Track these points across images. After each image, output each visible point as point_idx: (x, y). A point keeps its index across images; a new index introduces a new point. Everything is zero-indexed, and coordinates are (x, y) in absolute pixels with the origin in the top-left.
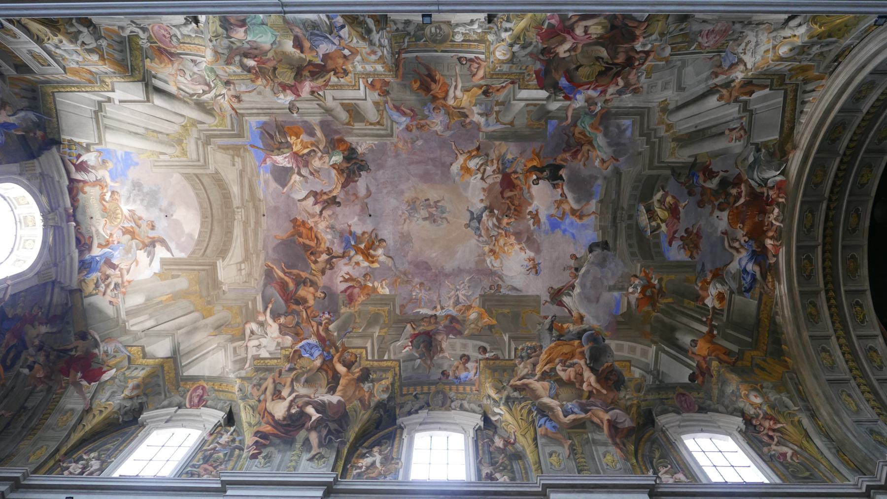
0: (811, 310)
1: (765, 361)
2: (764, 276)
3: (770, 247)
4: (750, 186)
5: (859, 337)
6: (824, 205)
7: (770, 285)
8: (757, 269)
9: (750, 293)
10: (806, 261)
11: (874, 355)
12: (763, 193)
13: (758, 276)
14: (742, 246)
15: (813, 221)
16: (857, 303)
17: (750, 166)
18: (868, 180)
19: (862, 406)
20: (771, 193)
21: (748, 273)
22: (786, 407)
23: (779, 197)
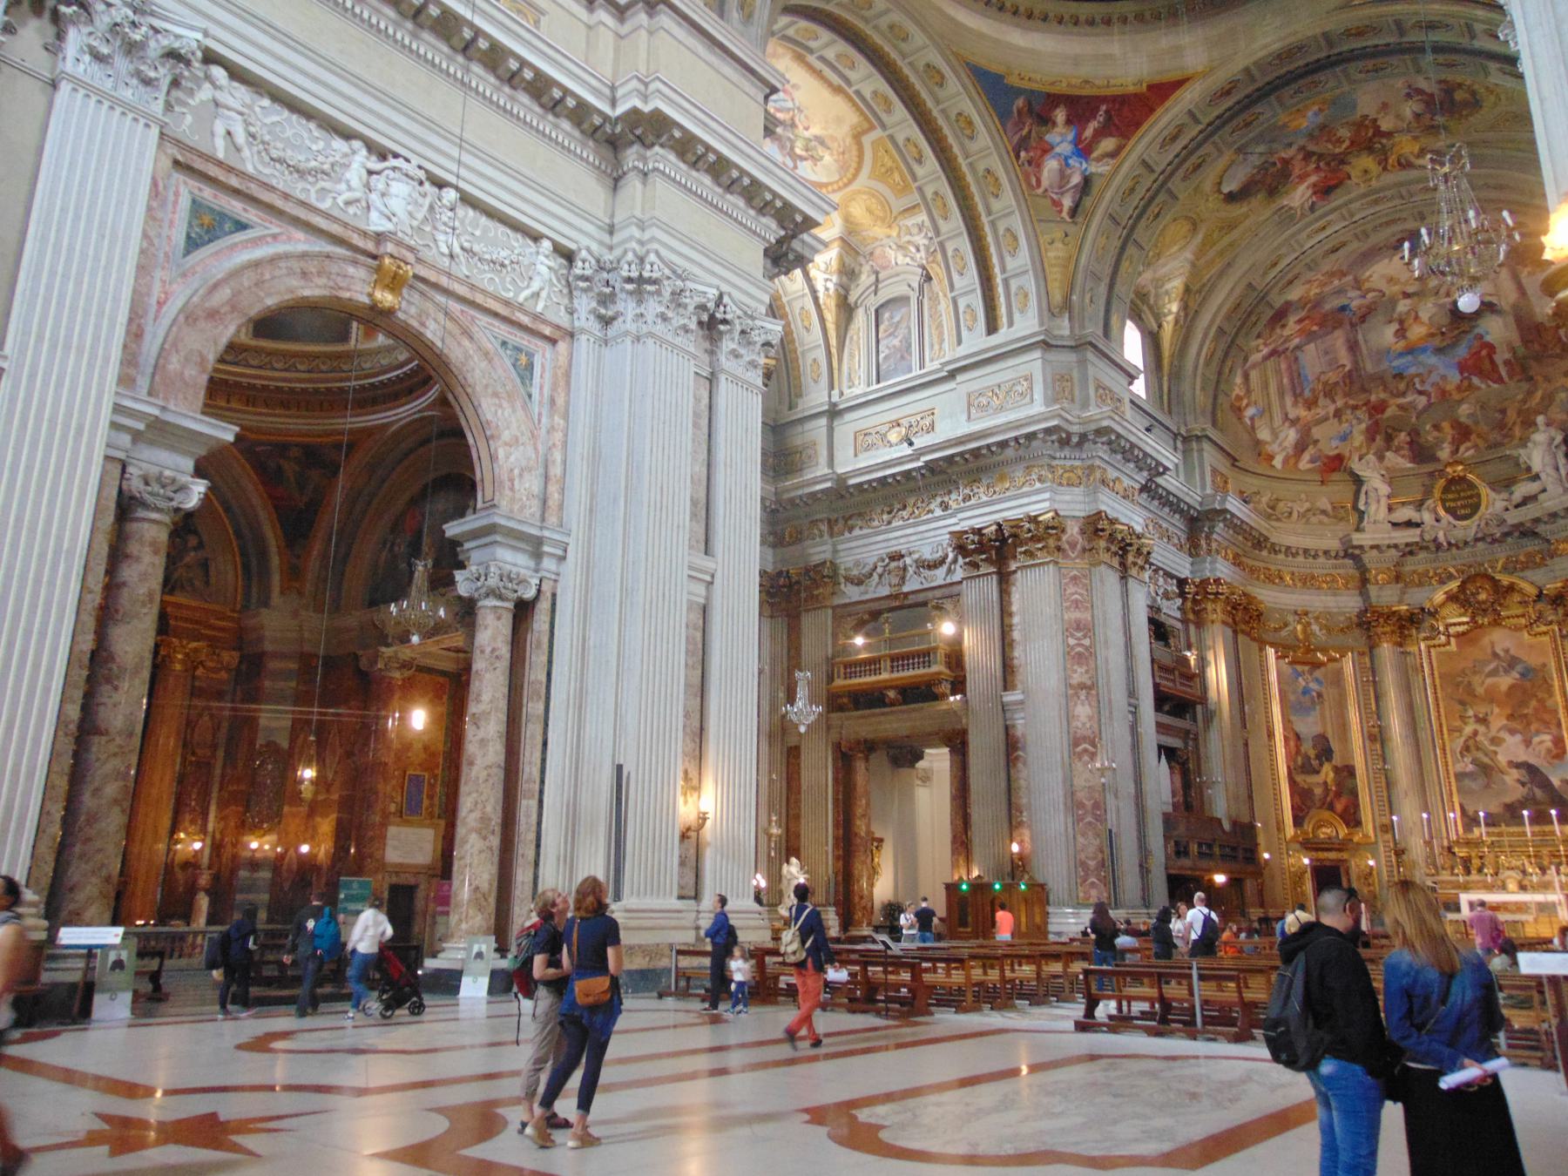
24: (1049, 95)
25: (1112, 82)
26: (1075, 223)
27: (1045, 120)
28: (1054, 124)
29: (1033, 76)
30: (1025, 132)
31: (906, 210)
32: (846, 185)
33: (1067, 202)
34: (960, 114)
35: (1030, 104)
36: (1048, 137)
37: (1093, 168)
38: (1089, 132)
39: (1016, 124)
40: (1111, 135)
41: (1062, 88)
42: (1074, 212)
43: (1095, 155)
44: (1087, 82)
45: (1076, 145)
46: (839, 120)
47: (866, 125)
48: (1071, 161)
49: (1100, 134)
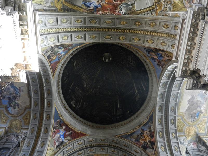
0: (79, 21)
1: (61, 3)
2: (89, 10)
3: (99, 13)
4: (120, 5)
5: (71, 35)
6: (113, 26)
7: (86, 12)
8: (92, 8)
9: (83, 4)
10: (95, 21)
11: (66, 38)
12: (117, 10)
13: (89, 8)
14: (99, 3)
15: (108, 24)
16: (82, 37)
17: (127, 3)
18: (121, 39)
19: (50, 24)
20: (117, 12)
21: (90, 5)
22: (46, 3)
23: (116, 14)
24: (64, 123)
25: (75, 128)
26: (56, 149)
27: (61, 127)
28: (62, 128)
29: (63, 118)
30: (57, 126)
31: (25, 128)
32: (16, 117)
33: (57, 144)
34: (48, 114)
35: (60, 122)
36: (60, 130)
37: (64, 141)
38: (67, 134)
39: (56, 123)
40: (70, 137)
41: (66, 123)
42: (57, 146)
43: (66, 138)
44: (71, 125)
45: (64, 135)
46: (25, 103)
47: (29, 107)
48: (61, 137)
49: (69, 135)
